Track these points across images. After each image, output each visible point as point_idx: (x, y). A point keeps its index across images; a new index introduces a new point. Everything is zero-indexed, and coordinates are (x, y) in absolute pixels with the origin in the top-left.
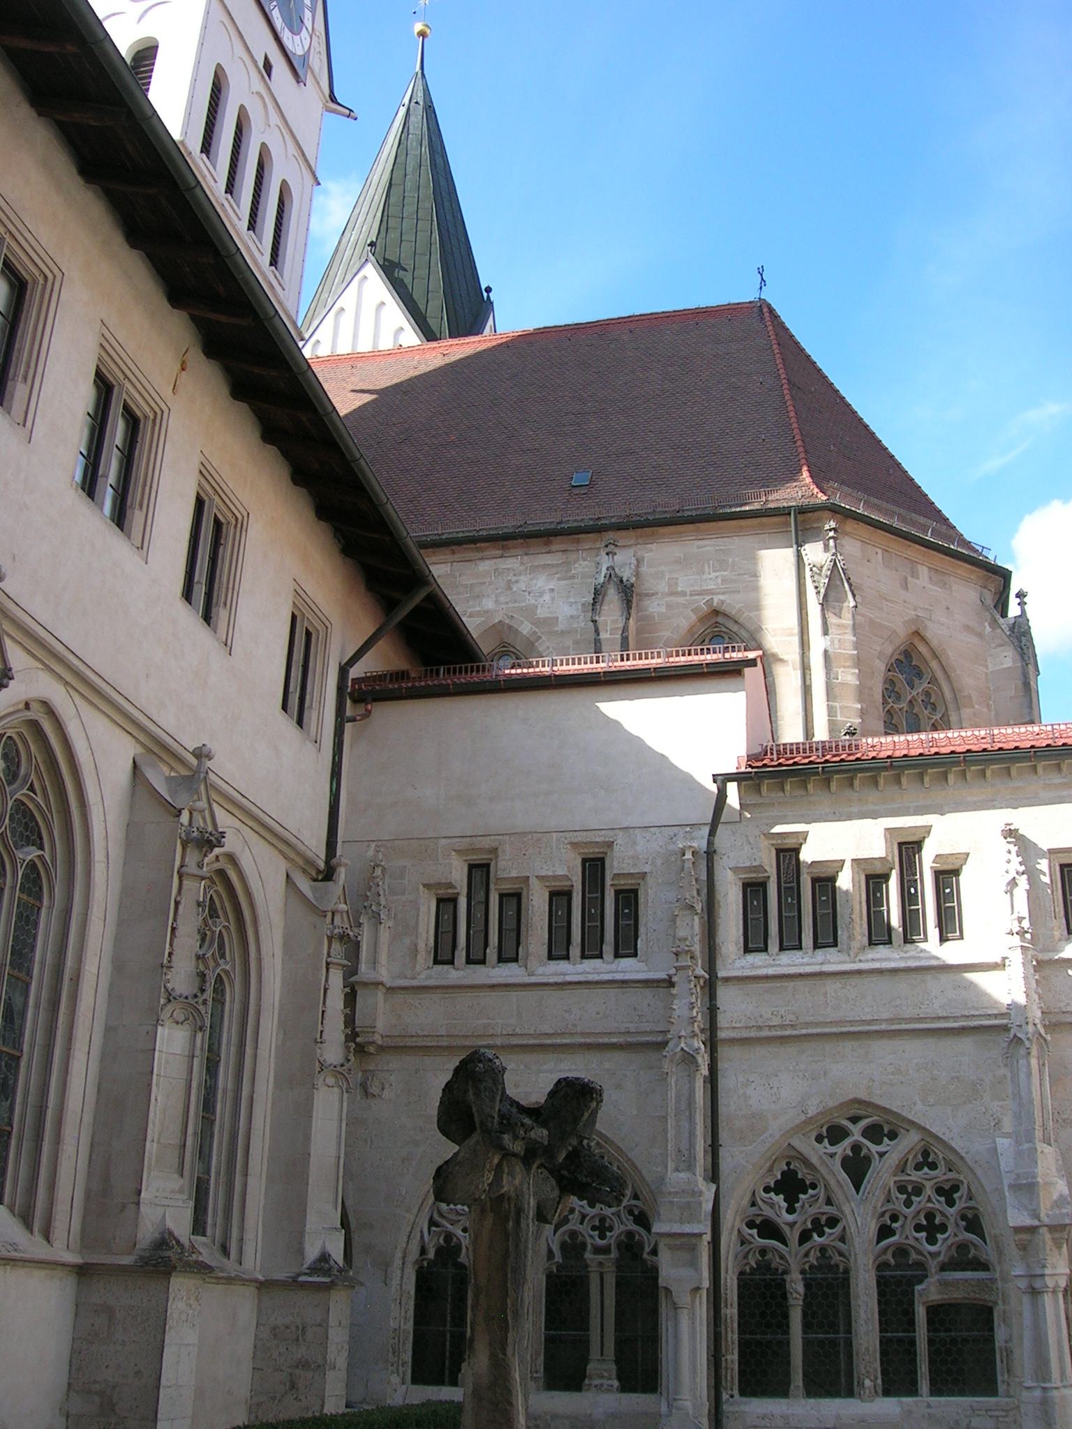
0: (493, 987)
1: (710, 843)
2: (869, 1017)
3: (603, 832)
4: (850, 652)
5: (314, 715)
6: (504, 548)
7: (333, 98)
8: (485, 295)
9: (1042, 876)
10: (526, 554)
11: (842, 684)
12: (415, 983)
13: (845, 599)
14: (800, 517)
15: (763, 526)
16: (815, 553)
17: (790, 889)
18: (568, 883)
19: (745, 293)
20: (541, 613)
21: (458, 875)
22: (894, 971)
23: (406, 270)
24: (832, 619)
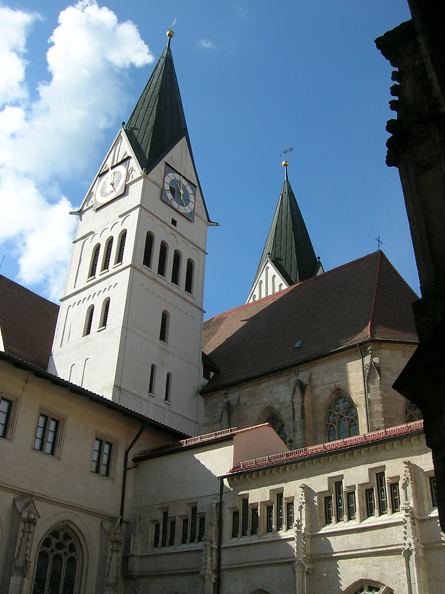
0: (165, 554)
1: (221, 500)
2: (262, 559)
3: (195, 499)
4: (380, 398)
5: (112, 470)
6: (269, 378)
7: (209, 221)
8: (318, 260)
9: (315, 503)
10: (276, 378)
11: (376, 411)
12: (146, 554)
13: (375, 377)
14: (361, 347)
15: (351, 352)
16: (367, 360)
17: (245, 514)
18: (187, 517)
19: (373, 249)
20: (281, 400)
21: (160, 517)
22: (270, 542)
23: (283, 260)
24: (371, 386)
